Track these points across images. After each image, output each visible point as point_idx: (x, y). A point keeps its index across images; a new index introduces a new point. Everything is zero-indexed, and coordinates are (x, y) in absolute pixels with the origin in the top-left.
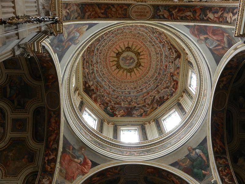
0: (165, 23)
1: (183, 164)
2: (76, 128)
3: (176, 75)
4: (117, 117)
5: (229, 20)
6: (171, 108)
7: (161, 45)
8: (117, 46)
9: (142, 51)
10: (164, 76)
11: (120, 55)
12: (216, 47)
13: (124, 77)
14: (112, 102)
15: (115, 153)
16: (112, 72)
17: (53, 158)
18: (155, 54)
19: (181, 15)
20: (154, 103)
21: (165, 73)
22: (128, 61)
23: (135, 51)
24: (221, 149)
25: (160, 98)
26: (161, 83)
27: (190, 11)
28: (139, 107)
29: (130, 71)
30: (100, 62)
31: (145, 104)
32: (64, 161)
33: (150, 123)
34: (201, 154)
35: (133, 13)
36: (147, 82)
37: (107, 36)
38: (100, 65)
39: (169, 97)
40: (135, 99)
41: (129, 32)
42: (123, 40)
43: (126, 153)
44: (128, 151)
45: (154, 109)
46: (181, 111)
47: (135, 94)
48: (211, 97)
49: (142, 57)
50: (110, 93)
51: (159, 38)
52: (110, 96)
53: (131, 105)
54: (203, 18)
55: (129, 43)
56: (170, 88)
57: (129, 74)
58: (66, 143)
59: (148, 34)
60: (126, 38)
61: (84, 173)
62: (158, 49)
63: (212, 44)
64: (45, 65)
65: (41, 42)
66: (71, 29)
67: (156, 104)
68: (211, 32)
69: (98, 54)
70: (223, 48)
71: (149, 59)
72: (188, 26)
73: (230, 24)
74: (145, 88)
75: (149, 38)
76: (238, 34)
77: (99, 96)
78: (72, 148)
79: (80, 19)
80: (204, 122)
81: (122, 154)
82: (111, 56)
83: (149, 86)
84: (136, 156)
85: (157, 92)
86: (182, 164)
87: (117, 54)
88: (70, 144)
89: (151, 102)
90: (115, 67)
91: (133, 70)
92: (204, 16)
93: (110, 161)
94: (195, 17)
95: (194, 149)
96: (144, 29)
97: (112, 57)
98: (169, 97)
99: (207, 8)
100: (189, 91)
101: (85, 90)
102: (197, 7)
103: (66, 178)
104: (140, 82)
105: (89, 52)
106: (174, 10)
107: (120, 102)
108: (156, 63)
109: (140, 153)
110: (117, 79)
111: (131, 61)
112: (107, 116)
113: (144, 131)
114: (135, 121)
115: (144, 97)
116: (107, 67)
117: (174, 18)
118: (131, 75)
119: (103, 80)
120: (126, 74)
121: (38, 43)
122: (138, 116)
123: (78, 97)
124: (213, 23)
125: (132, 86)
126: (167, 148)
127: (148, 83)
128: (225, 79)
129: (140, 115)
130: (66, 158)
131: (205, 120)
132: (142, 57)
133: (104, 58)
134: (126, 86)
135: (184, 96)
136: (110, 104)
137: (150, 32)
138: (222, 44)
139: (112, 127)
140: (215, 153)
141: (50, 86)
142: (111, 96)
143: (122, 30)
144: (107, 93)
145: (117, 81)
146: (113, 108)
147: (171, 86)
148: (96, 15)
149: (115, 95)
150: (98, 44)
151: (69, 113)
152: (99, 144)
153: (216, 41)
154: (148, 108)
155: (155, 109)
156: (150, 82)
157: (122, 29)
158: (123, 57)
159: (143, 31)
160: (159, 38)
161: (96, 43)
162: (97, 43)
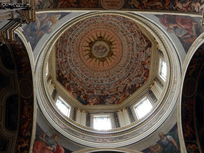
0: (136, 12)
1: (155, 150)
2: (49, 116)
3: (147, 64)
4: (90, 105)
5: (196, 9)
6: (143, 95)
7: (132, 35)
8: (89, 35)
9: (114, 41)
10: (135, 65)
11: (93, 45)
12: (184, 35)
13: (96, 66)
14: (85, 91)
15: (88, 141)
16: (85, 62)
17: (26, 146)
18: (127, 43)
19: (151, 5)
20: (126, 91)
21: (137, 62)
22: (100, 50)
23: (107, 40)
25: (132, 86)
26: (133, 72)
27: (160, 1)
28: (112, 95)
29: (103, 60)
30: (73, 51)
31: (117, 92)
32: (37, 149)
33: (122, 110)
34: (172, 140)
35: (105, 3)
36: (120, 70)
37: (80, 26)
38: (73, 54)
39: (140, 85)
40: (107, 88)
41: (101, 22)
42: (96, 29)
43: (99, 140)
44: (101, 138)
45: (126, 97)
46: (153, 99)
47: (108, 82)
48: (181, 84)
49: (114, 46)
50: (83, 82)
51: (130, 28)
52: (83, 84)
53: (104, 93)
54: (172, 8)
55: (101, 33)
56: (141, 76)
57: (101, 63)
58: (39, 129)
59: (120, 24)
60: (98, 28)
62: (130, 39)
63: (181, 33)
64: (18, 53)
65: (14, 30)
66: (43, 18)
67: (128, 92)
69: (72, 43)
70: (192, 37)
71: (121, 47)
72: (157, 16)
73: (198, 13)
74: (117, 77)
75: (120, 28)
77: (72, 84)
78: (44, 136)
79: (52, 8)
80: (175, 108)
81: (95, 141)
82: (84, 45)
83: (121, 74)
84: (109, 143)
85: (129, 80)
86: (154, 150)
87: (90, 44)
88: (43, 132)
89: (123, 90)
90: (88, 56)
91: (106, 59)
92: (173, 5)
93: (83, 148)
94: (164, 7)
95: (165, 135)
96: (116, 20)
98: (140, 85)
100: (160, 78)
101: (58, 79)
104: (112, 71)
105: (62, 41)
107: (92, 91)
108: (128, 52)
109: (113, 140)
110: (89, 68)
111: (104, 50)
112: (80, 105)
113: (116, 118)
114: (108, 109)
115: (116, 85)
116: (80, 57)
117: (144, 8)
118: (103, 64)
119: (76, 69)
120: (98, 63)
121: (11, 31)
122: (110, 104)
123: (52, 85)
124: (182, 13)
125: (105, 75)
126: (139, 135)
127: (120, 72)
128: (194, 67)
129: (113, 103)
130: (39, 146)
131: (175, 107)
132: (114, 46)
133: (77, 48)
134: (99, 74)
135: (155, 83)
136: (82, 92)
137: (121, 22)
138: (191, 33)
139: (85, 115)
140: (186, 139)
141: (23, 74)
142: (84, 84)
143: (94, 20)
144: (80, 82)
145: (90, 70)
146: (86, 97)
147: (143, 74)
148: (69, 5)
149: (88, 84)
150: (71, 33)
151: (42, 101)
152: (72, 132)
154: (120, 96)
155: (126, 97)
156: (122, 70)
157: (95, 19)
158: (96, 47)
159: (115, 21)
160: (130, 28)
161: (69, 33)
162: (70, 32)
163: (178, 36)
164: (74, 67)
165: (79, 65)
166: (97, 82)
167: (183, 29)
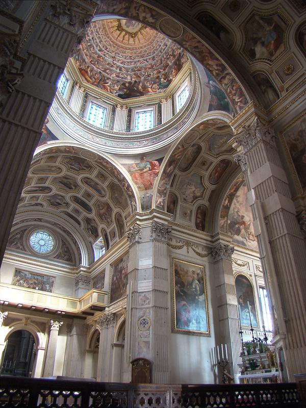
8: (108, 26)
24: (219, 68)
37: (89, 34)
61: (157, 174)
77: (145, 80)
82: (117, 37)
87: (118, 29)
90: (131, 39)
97: (119, 36)
103: (146, 189)
110: (145, 46)
116: (126, 49)
119: (135, 63)
128: (144, 15)
149: (158, 61)
162: (92, 49)
164: (133, 63)
165: (134, 55)
166: (162, 51)
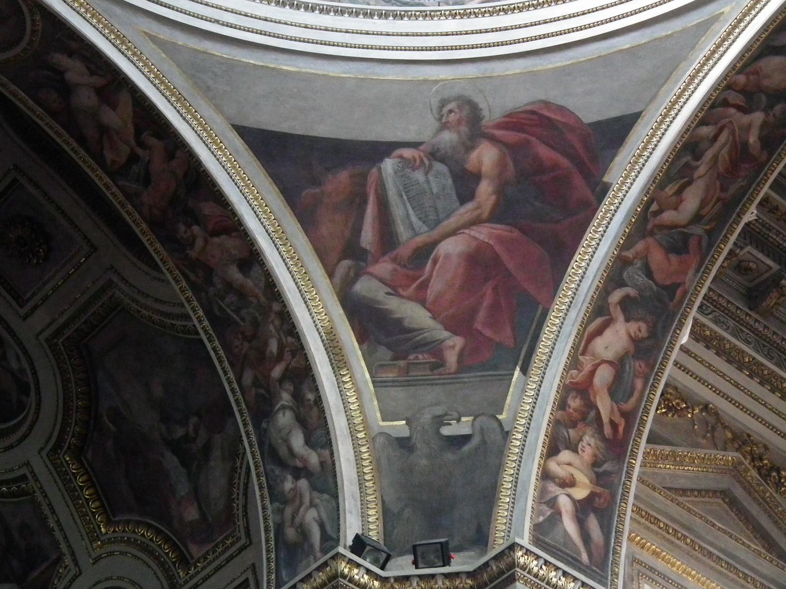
12: (383, 205)
19: (709, 155)
27: (697, 218)
54: (622, 284)
68: (505, 257)
76: (524, 568)
94: (652, 234)
99: (660, 326)
102: (691, 272)
106: (764, 125)
117: (725, 103)
128: (111, 117)
153: (420, 240)
163: (399, 152)
167: (435, 234)
